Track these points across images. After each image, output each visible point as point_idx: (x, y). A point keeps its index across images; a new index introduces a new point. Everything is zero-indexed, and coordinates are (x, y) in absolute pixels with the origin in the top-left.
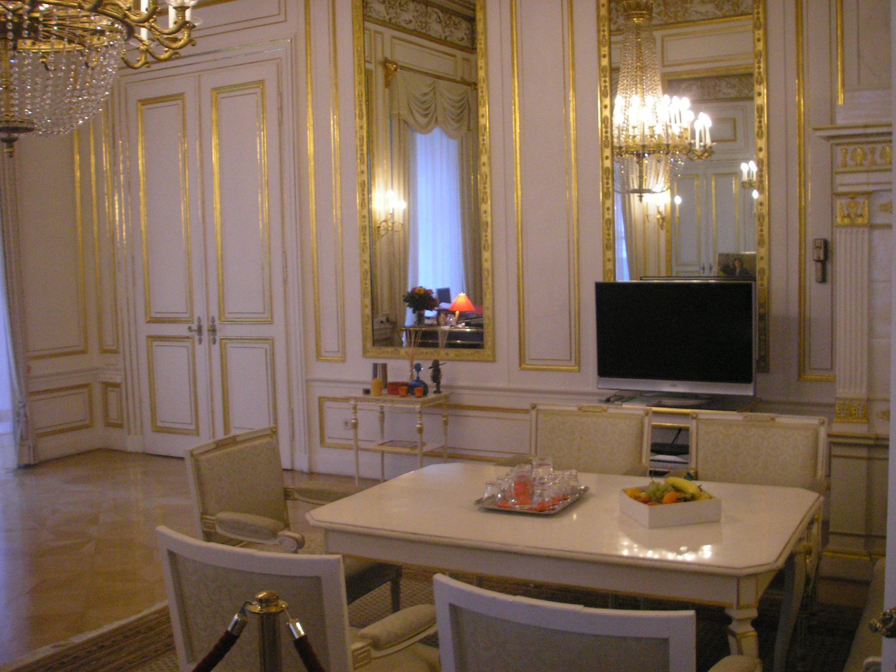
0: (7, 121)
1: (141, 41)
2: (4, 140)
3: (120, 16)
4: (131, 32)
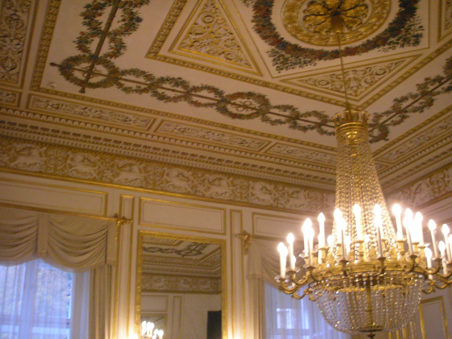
0: (371, 327)
1: (430, 280)
2: (369, 336)
3: (422, 272)
4: (426, 277)
